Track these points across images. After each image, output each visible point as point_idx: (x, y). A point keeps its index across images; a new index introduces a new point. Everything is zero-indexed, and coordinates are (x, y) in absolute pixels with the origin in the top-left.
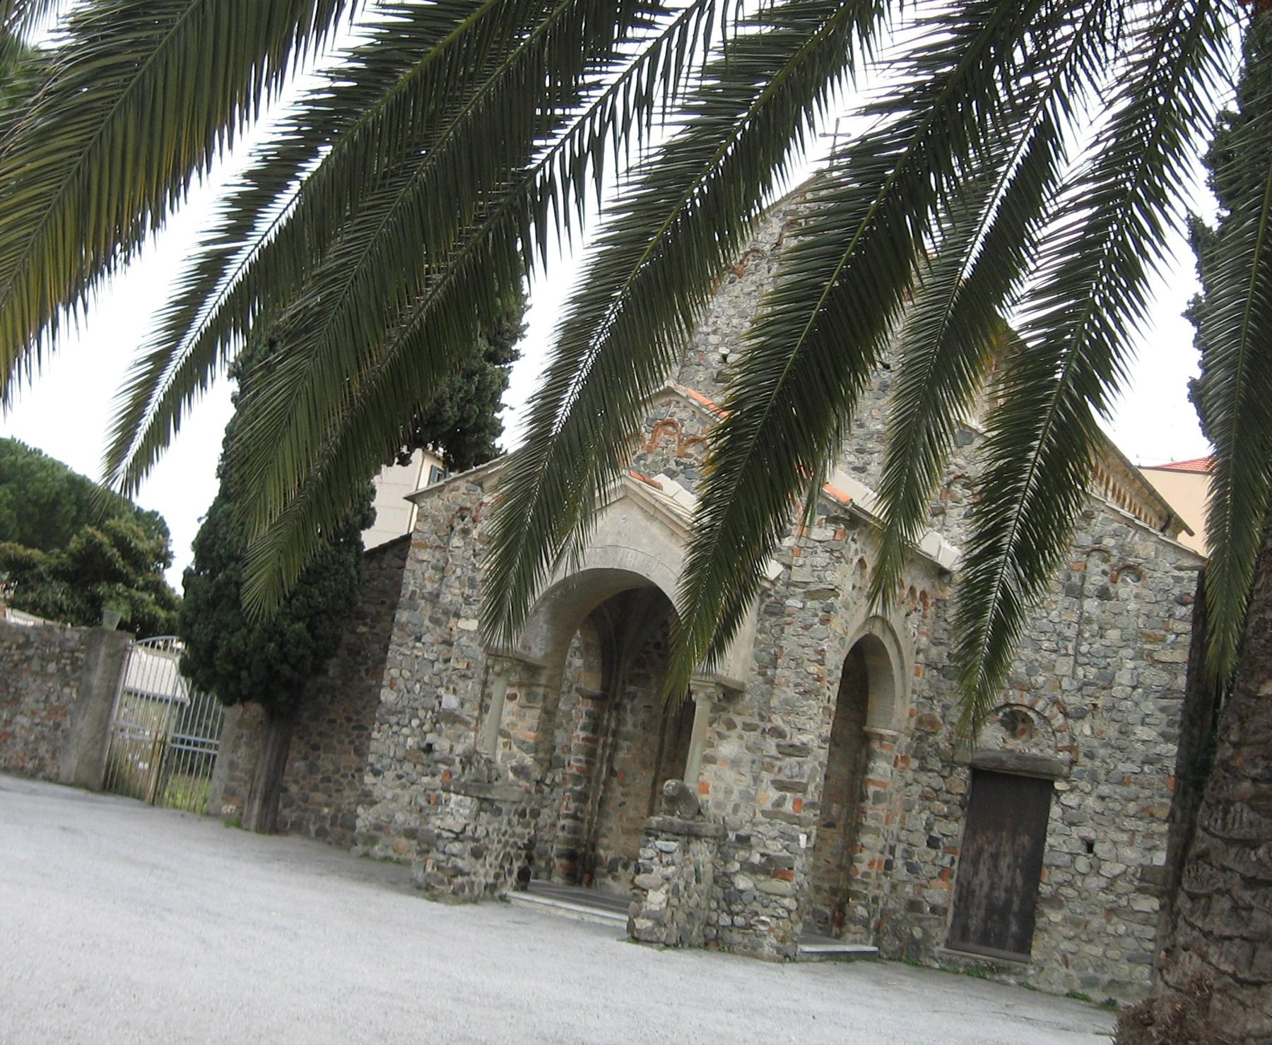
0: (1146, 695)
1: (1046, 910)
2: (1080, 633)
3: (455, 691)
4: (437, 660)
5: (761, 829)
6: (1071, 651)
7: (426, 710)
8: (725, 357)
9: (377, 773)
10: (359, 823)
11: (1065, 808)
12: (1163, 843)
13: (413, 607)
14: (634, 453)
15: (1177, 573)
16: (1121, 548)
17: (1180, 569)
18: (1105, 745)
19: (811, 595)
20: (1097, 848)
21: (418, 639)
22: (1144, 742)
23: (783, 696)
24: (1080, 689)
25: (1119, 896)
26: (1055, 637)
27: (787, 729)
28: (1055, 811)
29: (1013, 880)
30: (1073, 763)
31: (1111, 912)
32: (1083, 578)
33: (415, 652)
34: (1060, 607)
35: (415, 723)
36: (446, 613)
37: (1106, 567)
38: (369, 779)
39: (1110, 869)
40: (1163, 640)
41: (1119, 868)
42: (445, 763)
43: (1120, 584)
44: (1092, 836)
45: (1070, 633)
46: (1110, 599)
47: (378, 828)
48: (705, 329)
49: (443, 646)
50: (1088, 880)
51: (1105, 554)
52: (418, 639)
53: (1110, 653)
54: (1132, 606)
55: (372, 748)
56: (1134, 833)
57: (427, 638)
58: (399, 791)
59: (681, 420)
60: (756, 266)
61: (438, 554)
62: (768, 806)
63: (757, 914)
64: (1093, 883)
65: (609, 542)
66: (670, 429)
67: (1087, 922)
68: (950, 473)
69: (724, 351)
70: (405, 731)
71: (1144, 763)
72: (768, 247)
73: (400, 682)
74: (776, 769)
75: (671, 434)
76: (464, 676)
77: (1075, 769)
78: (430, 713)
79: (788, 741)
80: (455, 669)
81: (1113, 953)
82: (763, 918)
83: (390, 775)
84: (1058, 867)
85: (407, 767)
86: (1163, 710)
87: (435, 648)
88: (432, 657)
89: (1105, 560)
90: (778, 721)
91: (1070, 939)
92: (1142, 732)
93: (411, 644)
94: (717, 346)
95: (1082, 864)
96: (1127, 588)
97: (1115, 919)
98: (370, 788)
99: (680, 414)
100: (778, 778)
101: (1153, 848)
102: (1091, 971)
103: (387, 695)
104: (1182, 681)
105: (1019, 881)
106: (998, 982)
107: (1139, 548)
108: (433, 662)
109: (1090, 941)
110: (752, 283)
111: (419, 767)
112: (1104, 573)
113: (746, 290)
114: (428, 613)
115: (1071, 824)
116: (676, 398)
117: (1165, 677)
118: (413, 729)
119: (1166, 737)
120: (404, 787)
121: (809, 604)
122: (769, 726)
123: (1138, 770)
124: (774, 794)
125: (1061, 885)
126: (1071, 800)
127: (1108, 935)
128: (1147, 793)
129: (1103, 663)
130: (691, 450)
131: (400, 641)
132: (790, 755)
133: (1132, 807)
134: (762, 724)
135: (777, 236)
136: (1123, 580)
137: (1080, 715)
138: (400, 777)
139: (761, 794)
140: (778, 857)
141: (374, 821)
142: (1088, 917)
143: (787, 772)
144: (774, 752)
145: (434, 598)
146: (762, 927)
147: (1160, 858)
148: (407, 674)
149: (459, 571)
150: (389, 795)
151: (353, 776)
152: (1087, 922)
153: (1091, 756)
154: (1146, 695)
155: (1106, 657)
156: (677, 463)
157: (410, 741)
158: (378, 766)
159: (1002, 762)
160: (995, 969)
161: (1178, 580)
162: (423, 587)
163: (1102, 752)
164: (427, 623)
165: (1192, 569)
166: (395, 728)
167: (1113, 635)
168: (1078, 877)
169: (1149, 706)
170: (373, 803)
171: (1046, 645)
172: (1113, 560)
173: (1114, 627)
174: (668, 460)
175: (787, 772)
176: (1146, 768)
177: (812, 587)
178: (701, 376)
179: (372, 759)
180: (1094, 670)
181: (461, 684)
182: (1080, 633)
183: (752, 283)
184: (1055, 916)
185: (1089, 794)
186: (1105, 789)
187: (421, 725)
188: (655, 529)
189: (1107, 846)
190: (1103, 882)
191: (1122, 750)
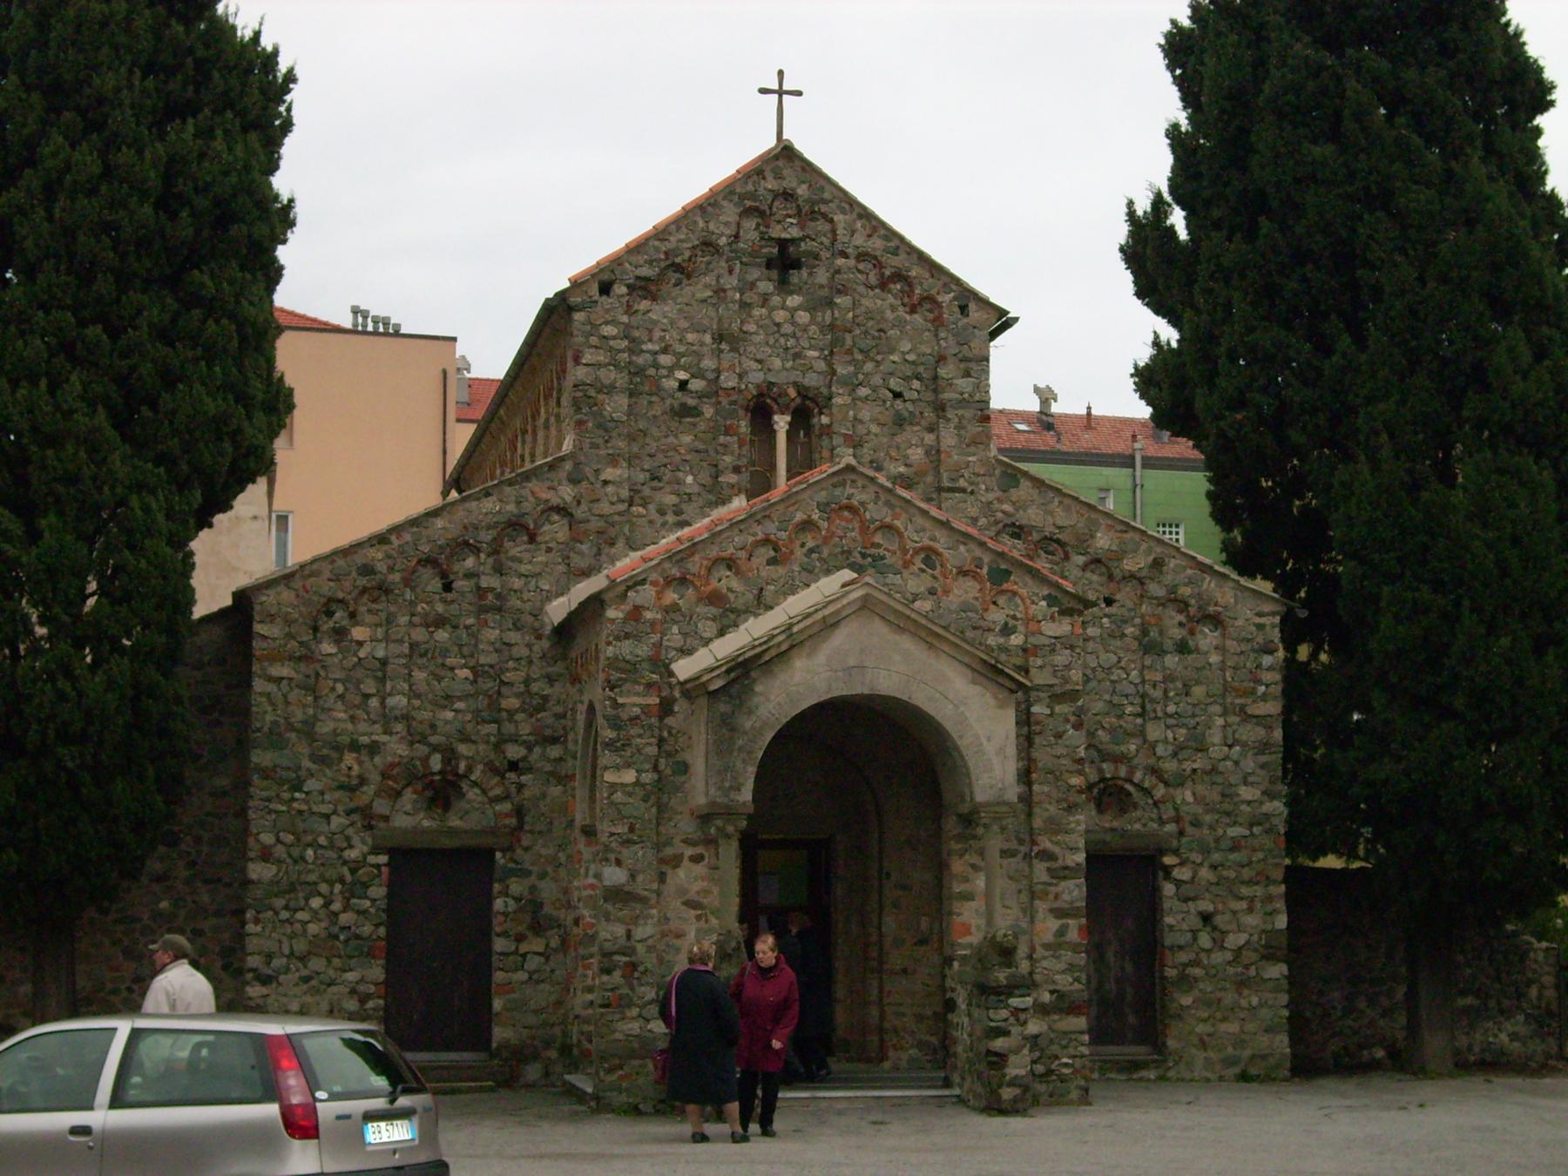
0: (1243, 754)
1: (1176, 995)
2: (1166, 692)
3: (619, 863)
4: (335, 812)
5: (1045, 964)
6: (1160, 714)
7: (331, 883)
8: (683, 385)
9: (265, 980)
11: (1179, 883)
12: (1280, 905)
13: (276, 739)
14: (803, 545)
15: (1258, 620)
16: (1199, 596)
17: (1260, 615)
18: (1207, 812)
19: (1056, 698)
20: (1219, 920)
22: (1249, 803)
23: (1046, 814)
24: (1175, 754)
25: (1247, 967)
26: (1137, 701)
27: (1056, 849)
28: (1169, 889)
29: (1123, 968)
30: (1181, 833)
31: (1242, 984)
32: (1161, 633)
33: (295, 805)
34: (1139, 666)
35: (316, 903)
36: (338, 748)
37: (1181, 618)
39: (1235, 940)
40: (1253, 692)
41: (1242, 938)
42: (624, 954)
43: (1199, 636)
44: (1211, 908)
45: (1157, 694)
46: (1190, 652)
48: (650, 346)
49: (339, 794)
50: (1213, 956)
51: (1182, 606)
52: (297, 786)
53: (1197, 711)
54: (1214, 659)
56: (1252, 899)
57: (312, 785)
58: (308, 999)
59: (862, 504)
60: (709, 263)
61: (302, 666)
62: (1049, 937)
63: (1057, 1057)
64: (1218, 957)
65: (852, 662)
66: (846, 513)
67: (1220, 1000)
68: (997, 523)
69: (682, 375)
70: (300, 915)
71: (1251, 825)
72: (723, 241)
73: (280, 851)
74: (1051, 897)
75: (848, 521)
76: (628, 842)
77: (1184, 840)
78: (338, 887)
79: (1060, 863)
80: (612, 834)
81: (1251, 1027)
82: (1065, 1060)
84: (1180, 948)
85: (317, 964)
86: (1262, 767)
87: (327, 797)
88: (325, 809)
89: (1180, 612)
90: (1045, 843)
91: (1205, 1021)
92: (1246, 793)
93: (286, 796)
94: (671, 369)
95: (1205, 940)
96: (1207, 638)
97: (1246, 992)
99: (859, 496)
100: (1056, 905)
101: (1275, 912)
102: (1230, 1050)
103: (258, 871)
104: (1278, 734)
105: (1129, 968)
106: (1141, 1079)
107: (1218, 596)
108: (327, 817)
109: (1224, 1019)
110: (706, 286)
111: (336, 961)
112: (1181, 624)
113: (699, 296)
114: (306, 751)
115: (1186, 900)
116: (853, 477)
117: (1262, 732)
118: (316, 912)
119: (1270, 795)
121: (1057, 709)
122: (1036, 849)
123: (1247, 833)
124: (1054, 924)
125: (1186, 965)
126: (1183, 874)
127: (1243, 1009)
128: (1260, 855)
129: (1193, 722)
130: (878, 539)
131: (265, 794)
132: (1065, 878)
133: (1247, 873)
134: (1023, 849)
135: (734, 227)
136: (1202, 632)
137: (1180, 781)
139: (1039, 926)
140: (1071, 992)
142: (1219, 995)
143: (1066, 897)
144: (1045, 877)
145: (308, 730)
146: (1066, 1071)
147: (1282, 921)
151: (130, 989)
152: (1220, 1000)
153: (1196, 824)
154: (1243, 754)
155: (1194, 716)
156: (864, 556)
157: (313, 928)
159: (1105, 842)
160: (1134, 1066)
161: (1260, 627)
163: (1208, 818)
164: (306, 763)
165: (1273, 614)
166: (284, 915)
167: (1199, 691)
168: (1203, 955)
169: (1249, 764)
171: (1129, 709)
172: (1192, 610)
173: (1198, 683)
174: (849, 552)
175: (1066, 897)
176: (1256, 830)
177: (1058, 690)
178: (657, 410)
179: (253, 961)
180: (1183, 731)
181: (626, 853)
182: (1166, 692)
183: (706, 286)
184: (1186, 1000)
185: (1201, 864)
186: (1216, 857)
187: (327, 904)
188: (907, 643)
189: (1228, 916)
190: (1229, 956)
191: (1228, 814)
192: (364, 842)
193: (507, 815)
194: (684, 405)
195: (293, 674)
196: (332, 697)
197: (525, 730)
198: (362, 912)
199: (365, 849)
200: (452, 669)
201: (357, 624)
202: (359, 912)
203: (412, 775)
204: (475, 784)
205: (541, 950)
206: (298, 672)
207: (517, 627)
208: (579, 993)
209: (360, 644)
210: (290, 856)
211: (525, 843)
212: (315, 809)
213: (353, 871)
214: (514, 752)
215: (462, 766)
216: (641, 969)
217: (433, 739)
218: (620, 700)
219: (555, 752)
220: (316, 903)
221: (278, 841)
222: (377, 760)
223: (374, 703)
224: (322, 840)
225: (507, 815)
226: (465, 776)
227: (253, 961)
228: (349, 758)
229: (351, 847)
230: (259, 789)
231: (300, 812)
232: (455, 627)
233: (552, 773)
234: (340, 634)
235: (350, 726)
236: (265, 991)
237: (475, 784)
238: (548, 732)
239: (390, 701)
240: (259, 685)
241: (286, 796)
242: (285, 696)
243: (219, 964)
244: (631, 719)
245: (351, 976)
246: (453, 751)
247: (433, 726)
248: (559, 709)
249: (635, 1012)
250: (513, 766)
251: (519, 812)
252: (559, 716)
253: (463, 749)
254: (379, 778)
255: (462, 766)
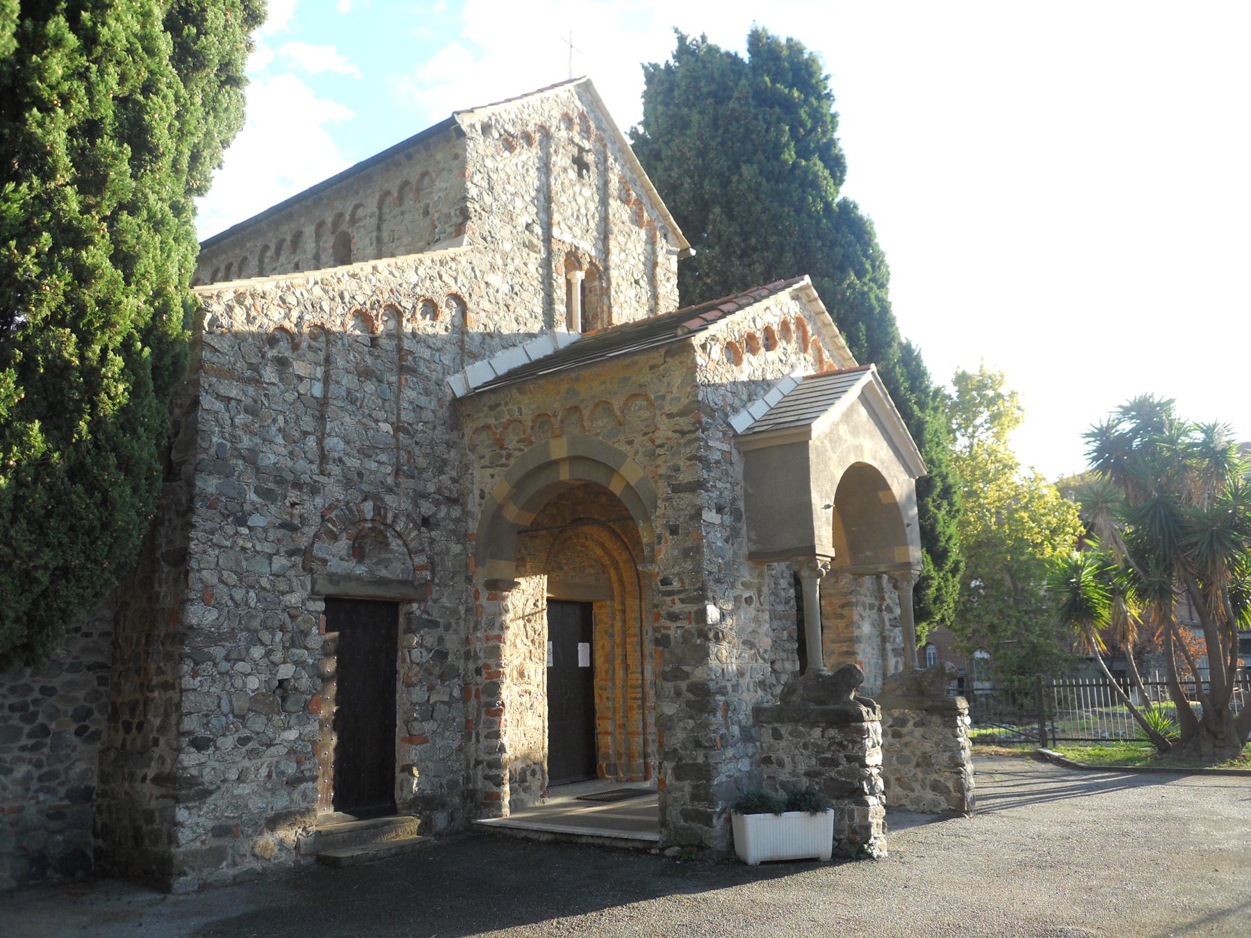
4: (277, 553)
9: (200, 744)
10: (184, 836)
21: (241, 521)
36: (280, 481)
38: (190, 759)
47: (221, 831)
49: (281, 533)
52: (241, 521)
55: (187, 706)
57: (256, 520)
58: (246, 763)
61: (251, 390)
70: (240, 666)
78: (279, 634)
83: (227, 742)
88: (268, 548)
98: (195, 772)
103: (200, 615)
108: (270, 557)
120: (253, 754)
131: (209, 525)
138: (243, 741)
141: (210, 824)
145: (251, 458)
148: (232, 579)
149: (281, 418)
150: (233, 775)
157: (253, 683)
158: (202, 733)
162: (234, 439)
164: (252, 496)
166: (225, 666)
170: (205, 794)
187: (268, 654)
192: (303, 587)
193: (423, 568)
194: (530, 241)
195: (241, 397)
196: (274, 429)
197: (431, 488)
198: (299, 663)
199: (305, 595)
200: (377, 421)
201: (299, 358)
202: (296, 663)
203: (351, 519)
204: (399, 535)
205: (446, 699)
206: (245, 394)
207: (427, 393)
208: (482, 739)
209: (300, 378)
210: (232, 598)
211: (434, 596)
212: (258, 548)
213: (293, 617)
214: (426, 508)
215: (390, 516)
216: (732, 708)
217: (365, 487)
218: (710, 443)
219: (456, 512)
220: (257, 652)
221: (221, 581)
222: (319, 501)
223: (311, 442)
224: (264, 582)
225: (423, 568)
226: (391, 526)
227: (190, 724)
228: (293, 495)
229: (292, 591)
230: (203, 518)
231: (244, 549)
232: (380, 381)
233: (453, 532)
234: (282, 363)
235: (290, 463)
236: (201, 757)
237: (399, 535)
238: (447, 494)
239: (330, 442)
240: (207, 401)
241: (230, 530)
242: (232, 419)
243: (73, 727)
244: (718, 462)
245: (292, 735)
246: (382, 500)
247: (360, 475)
248: (454, 474)
249: (730, 753)
250: (426, 522)
251: (432, 566)
252: (454, 481)
253: (388, 499)
254: (319, 520)
255: (390, 516)
